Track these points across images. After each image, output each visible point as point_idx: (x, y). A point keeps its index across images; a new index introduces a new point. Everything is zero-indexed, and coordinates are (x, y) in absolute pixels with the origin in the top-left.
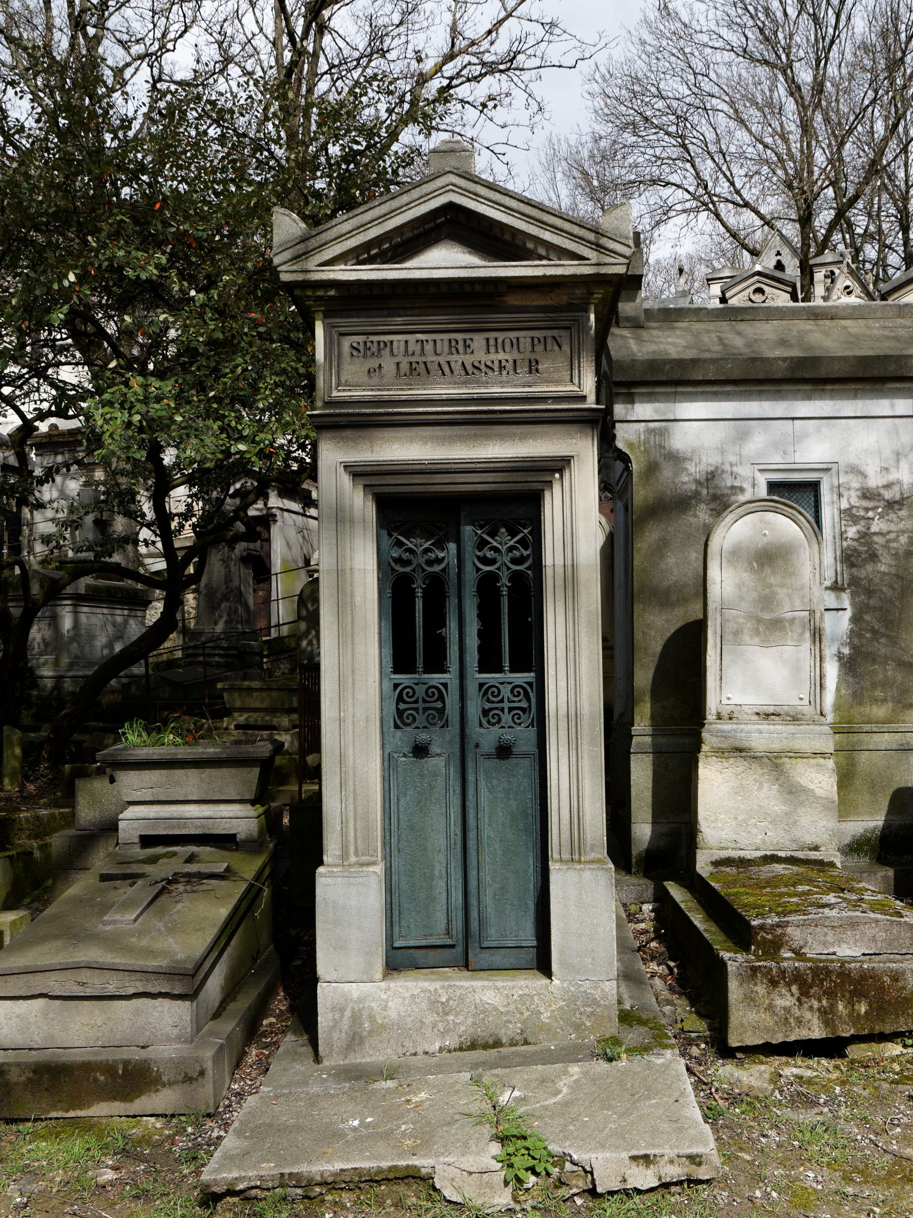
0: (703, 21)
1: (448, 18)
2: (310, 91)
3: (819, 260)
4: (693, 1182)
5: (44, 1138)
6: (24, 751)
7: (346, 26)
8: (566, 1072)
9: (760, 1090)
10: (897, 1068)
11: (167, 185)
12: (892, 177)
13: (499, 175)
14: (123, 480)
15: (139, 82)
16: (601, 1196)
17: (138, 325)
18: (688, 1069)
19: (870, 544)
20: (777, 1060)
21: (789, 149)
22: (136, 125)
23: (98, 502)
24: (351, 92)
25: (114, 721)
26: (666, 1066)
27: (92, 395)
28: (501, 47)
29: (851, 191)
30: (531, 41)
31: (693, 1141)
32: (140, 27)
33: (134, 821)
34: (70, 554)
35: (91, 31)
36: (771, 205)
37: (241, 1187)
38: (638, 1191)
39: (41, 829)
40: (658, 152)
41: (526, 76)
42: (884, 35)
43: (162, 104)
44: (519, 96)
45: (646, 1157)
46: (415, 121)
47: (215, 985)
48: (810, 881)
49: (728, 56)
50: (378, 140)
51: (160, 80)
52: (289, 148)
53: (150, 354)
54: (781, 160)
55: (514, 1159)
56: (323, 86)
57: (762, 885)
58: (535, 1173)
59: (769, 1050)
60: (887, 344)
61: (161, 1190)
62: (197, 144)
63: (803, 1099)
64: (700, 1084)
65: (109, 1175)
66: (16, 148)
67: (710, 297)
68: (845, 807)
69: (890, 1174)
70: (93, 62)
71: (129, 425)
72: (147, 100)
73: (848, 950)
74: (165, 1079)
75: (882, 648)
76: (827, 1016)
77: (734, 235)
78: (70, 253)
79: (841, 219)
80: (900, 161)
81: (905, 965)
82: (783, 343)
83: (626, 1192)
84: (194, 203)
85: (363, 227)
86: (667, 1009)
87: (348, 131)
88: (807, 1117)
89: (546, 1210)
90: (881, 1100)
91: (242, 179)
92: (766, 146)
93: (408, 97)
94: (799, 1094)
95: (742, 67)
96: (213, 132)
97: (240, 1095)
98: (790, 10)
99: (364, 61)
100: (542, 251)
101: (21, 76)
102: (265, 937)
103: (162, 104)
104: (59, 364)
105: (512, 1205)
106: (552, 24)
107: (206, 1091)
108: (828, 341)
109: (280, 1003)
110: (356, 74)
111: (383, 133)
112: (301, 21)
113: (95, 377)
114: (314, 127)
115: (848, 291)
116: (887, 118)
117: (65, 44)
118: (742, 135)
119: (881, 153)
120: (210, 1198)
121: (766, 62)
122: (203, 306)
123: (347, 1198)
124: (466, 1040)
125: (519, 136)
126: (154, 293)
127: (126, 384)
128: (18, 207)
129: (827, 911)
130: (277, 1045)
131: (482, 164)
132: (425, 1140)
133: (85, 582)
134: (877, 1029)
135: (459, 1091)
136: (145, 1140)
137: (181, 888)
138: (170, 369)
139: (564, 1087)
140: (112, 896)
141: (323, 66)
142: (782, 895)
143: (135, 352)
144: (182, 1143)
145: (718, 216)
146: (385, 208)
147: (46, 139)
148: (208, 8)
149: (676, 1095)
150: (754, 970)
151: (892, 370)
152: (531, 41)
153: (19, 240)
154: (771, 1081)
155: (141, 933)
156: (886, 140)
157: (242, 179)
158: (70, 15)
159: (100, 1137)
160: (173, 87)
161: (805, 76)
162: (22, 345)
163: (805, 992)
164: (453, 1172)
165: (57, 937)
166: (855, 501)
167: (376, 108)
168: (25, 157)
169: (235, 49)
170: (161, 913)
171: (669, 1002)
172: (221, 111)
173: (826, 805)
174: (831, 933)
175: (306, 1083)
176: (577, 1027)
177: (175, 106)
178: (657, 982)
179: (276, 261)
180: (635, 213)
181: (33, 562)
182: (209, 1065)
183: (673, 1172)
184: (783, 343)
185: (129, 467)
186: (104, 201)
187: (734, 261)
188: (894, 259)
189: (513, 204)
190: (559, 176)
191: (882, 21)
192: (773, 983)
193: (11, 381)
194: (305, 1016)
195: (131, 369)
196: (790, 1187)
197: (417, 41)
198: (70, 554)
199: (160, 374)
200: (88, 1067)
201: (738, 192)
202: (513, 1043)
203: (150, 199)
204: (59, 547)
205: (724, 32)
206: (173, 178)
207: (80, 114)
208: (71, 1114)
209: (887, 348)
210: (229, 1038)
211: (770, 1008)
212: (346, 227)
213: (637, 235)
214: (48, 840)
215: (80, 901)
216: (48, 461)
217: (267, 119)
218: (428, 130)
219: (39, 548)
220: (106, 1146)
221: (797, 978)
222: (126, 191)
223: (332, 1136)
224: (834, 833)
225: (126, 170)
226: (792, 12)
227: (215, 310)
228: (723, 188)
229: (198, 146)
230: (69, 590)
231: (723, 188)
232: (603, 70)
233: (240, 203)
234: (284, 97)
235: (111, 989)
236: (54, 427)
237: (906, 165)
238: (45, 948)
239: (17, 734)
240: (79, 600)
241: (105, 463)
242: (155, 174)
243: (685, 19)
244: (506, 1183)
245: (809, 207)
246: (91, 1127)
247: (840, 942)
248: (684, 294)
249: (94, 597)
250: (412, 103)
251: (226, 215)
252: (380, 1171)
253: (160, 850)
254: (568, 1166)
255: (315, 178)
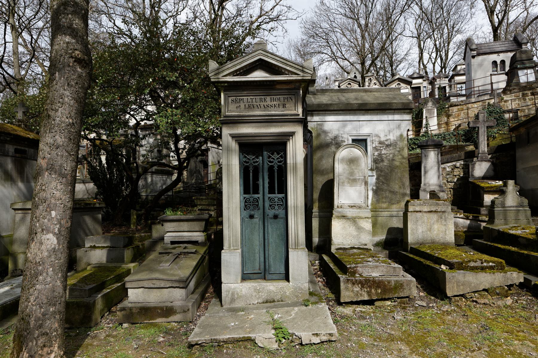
0: (333, 6)
1: (259, 5)
2: (220, 26)
3: (367, 75)
4: (330, 341)
5: (143, 328)
6: (137, 217)
7: (230, 7)
8: (294, 310)
9: (350, 315)
10: (389, 308)
11: (178, 54)
12: (388, 51)
13: (274, 50)
14: (165, 139)
15: (170, 24)
16: (304, 345)
17: (170, 94)
18: (329, 309)
19: (381, 157)
20: (355, 306)
21: (358, 43)
22: (169, 36)
23: (158, 145)
24: (232, 27)
25: (163, 208)
26: (323, 308)
27: (156, 114)
28: (275, 13)
29: (376, 55)
30: (284, 12)
31: (330, 329)
32: (170, 8)
33: (169, 237)
34: (150, 160)
35: (156, 9)
36: (353, 59)
37: (200, 342)
38: (315, 344)
39: (142, 239)
40: (320, 44)
41: (282, 22)
42: (385, 10)
43: (177, 30)
44: (280, 28)
45: (317, 334)
46: (250, 35)
47: (192, 284)
48: (364, 254)
49: (340, 16)
50: (240, 40)
51: (176, 23)
52: (214, 43)
53: (173, 102)
54: (356, 46)
55: (278, 335)
56: (223, 25)
57: (350, 255)
58: (285, 339)
59: (352, 303)
60: (386, 99)
61: (176, 343)
62: (187, 41)
63: (363, 318)
64: (332, 313)
65: (162, 339)
66: (135, 43)
67: (335, 86)
68: (374, 233)
69: (387, 339)
70: (157, 18)
71: (167, 123)
72: (172, 29)
73: (375, 274)
74: (178, 311)
75: (385, 187)
76: (369, 293)
77: (342, 68)
78: (150, 73)
79: (373, 63)
80: (390, 47)
81: (392, 278)
82: (356, 99)
83: (311, 344)
84: (186, 58)
85: (235, 66)
86: (323, 291)
87: (231, 38)
88: (363, 322)
89: (288, 349)
90: (385, 317)
91: (200, 52)
92: (351, 42)
93: (248, 28)
94: (361, 316)
95: (344, 20)
96: (192, 38)
97: (199, 316)
98: (358, 3)
99: (235, 18)
100: (287, 72)
101: (136, 22)
102: (206, 271)
103: (177, 30)
104: (147, 105)
105: (278, 348)
106: (290, 7)
107: (189, 315)
108: (369, 98)
109: (211, 289)
110: (233, 21)
111: (241, 38)
112: (217, 6)
113: (157, 109)
114: (221, 37)
115: (375, 84)
116: (386, 34)
117: (149, 13)
118: (344, 39)
119: (385, 44)
120: (191, 346)
121: (352, 18)
122: (189, 88)
123: (230, 346)
124: (265, 300)
125: (280, 39)
126: (174, 85)
127: (167, 111)
128: (135, 60)
129: (369, 263)
130: (210, 301)
131: (269, 47)
132: (253, 329)
133: (155, 168)
134: (384, 297)
135: (263, 315)
136: (172, 329)
137: (182, 256)
138: (179, 107)
139: (293, 314)
140: (162, 259)
141: (223, 19)
142: (356, 258)
143: (169, 102)
144: (183, 330)
145: (337, 62)
146: (241, 60)
147: (143, 40)
148: (190, 2)
149: (325, 316)
150: (348, 280)
151: (388, 107)
152: (284, 12)
153: (136, 69)
154: (353, 312)
155: (171, 269)
156: (386, 40)
157: (200, 52)
158: (150, 4)
159: (159, 328)
160: (180, 25)
161: (363, 22)
162: (136, 100)
163: (363, 286)
164: (261, 338)
165: (146, 270)
166: (377, 145)
167: (239, 31)
168: (137, 45)
169: (198, 14)
170: (177, 263)
171: (323, 289)
172: (194, 32)
173: (369, 232)
174: (370, 269)
175: (218, 313)
176: (297, 296)
177: (180, 30)
178: (320, 283)
179: (210, 75)
180: (313, 61)
181: (140, 162)
182: (190, 307)
183: (325, 338)
184: (356, 99)
185: (167, 135)
186: (160, 58)
187: (342, 75)
188: (388, 75)
189: (278, 59)
190: (292, 51)
191: (385, 6)
192: (354, 284)
193: (133, 110)
194: (218, 293)
195: (168, 107)
196: (359, 343)
197: (251, 12)
198: (150, 160)
199: (176, 108)
200: (155, 308)
201: (343, 55)
202: (278, 301)
203: (173, 58)
204: (147, 158)
205: (339, 9)
206: (180, 51)
207: (153, 33)
208: (151, 321)
209: (386, 100)
210: (196, 299)
211: (353, 291)
212: (230, 66)
213: (314, 68)
214: (144, 242)
215: (153, 260)
216: (144, 133)
217: (207, 34)
218: (254, 38)
219: (141, 158)
220: (161, 331)
221: (360, 282)
222: (166, 55)
223: (226, 328)
224: (371, 241)
225: (166, 49)
226: (359, 3)
227: (192, 90)
228: (339, 54)
229: (187, 42)
230: (150, 170)
231: (339, 54)
232: (304, 20)
233: (199, 58)
234: (212, 28)
235: (162, 286)
236: (145, 123)
237: (392, 48)
238: (143, 273)
239: (135, 212)
240: (153, 173)
241: (160, 134)
242: (175, 50)
243: (328, 6)
244: (276, 342)
245: (364, 60)
246: (156, 325)
247: (373, 272)
248: (328, 85)
249: (157, 172)
250: (249, 30)
251: (195, 62)
252: (240, 338)
253: (176, 245)
254: (294, 337)
255: (221, 51)
